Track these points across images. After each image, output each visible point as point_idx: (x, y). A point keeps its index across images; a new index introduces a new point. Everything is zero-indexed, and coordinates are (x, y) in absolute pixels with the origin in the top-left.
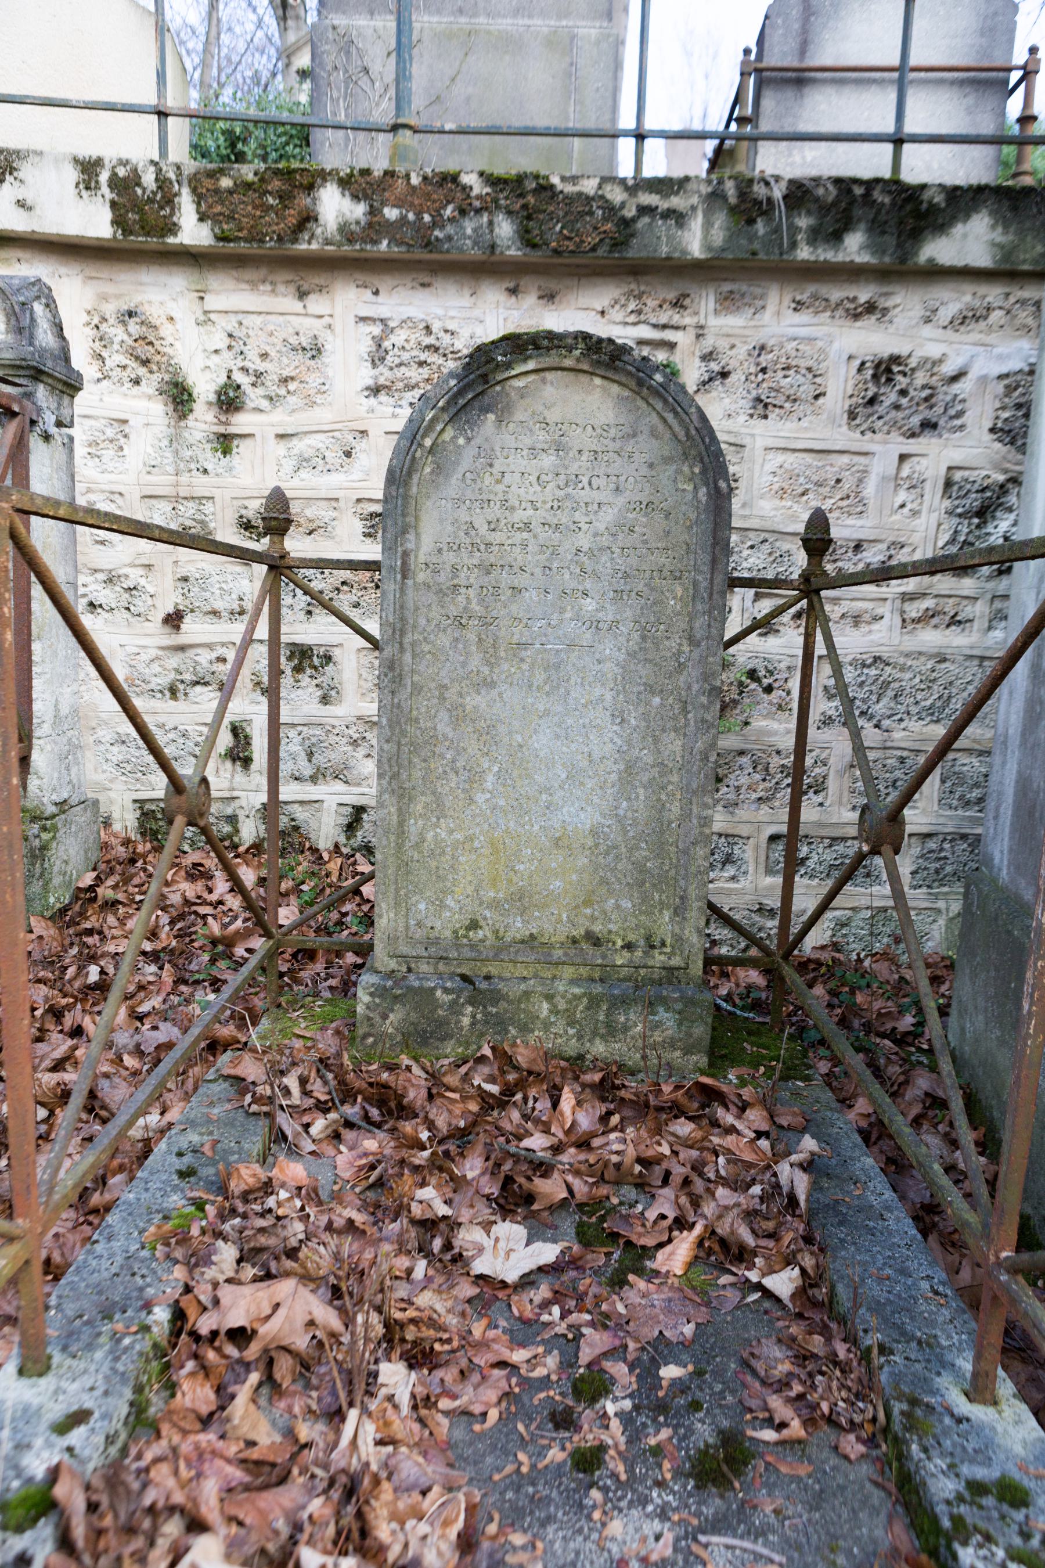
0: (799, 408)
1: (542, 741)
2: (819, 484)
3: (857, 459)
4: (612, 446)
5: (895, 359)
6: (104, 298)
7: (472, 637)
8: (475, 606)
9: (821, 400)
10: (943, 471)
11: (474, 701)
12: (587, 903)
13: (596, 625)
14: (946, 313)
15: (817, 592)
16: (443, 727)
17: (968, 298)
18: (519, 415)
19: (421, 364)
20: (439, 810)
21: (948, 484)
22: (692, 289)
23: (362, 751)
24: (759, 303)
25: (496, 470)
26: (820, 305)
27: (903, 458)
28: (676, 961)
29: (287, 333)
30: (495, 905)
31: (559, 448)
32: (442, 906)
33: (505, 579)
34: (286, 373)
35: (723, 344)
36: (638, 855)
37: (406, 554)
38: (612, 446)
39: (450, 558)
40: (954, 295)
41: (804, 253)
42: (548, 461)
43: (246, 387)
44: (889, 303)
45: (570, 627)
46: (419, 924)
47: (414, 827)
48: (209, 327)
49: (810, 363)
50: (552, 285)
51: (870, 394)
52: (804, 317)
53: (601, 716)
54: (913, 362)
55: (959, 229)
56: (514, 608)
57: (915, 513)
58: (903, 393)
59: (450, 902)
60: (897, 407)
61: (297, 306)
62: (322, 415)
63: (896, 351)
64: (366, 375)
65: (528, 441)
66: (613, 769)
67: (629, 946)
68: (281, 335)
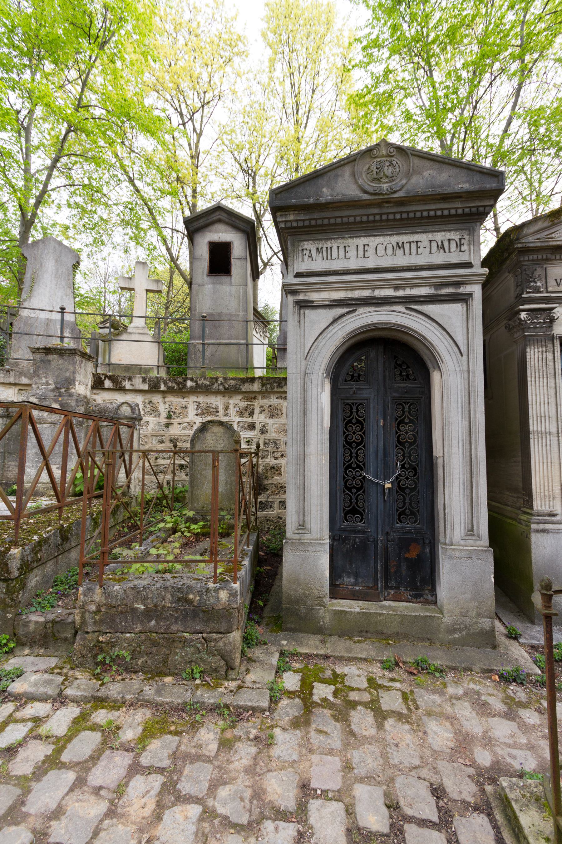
16: (199, 476)
22: (257, 395)
31: (215, 436)
41: (276, 390)
47: (194, 492)
64: (195, 412)
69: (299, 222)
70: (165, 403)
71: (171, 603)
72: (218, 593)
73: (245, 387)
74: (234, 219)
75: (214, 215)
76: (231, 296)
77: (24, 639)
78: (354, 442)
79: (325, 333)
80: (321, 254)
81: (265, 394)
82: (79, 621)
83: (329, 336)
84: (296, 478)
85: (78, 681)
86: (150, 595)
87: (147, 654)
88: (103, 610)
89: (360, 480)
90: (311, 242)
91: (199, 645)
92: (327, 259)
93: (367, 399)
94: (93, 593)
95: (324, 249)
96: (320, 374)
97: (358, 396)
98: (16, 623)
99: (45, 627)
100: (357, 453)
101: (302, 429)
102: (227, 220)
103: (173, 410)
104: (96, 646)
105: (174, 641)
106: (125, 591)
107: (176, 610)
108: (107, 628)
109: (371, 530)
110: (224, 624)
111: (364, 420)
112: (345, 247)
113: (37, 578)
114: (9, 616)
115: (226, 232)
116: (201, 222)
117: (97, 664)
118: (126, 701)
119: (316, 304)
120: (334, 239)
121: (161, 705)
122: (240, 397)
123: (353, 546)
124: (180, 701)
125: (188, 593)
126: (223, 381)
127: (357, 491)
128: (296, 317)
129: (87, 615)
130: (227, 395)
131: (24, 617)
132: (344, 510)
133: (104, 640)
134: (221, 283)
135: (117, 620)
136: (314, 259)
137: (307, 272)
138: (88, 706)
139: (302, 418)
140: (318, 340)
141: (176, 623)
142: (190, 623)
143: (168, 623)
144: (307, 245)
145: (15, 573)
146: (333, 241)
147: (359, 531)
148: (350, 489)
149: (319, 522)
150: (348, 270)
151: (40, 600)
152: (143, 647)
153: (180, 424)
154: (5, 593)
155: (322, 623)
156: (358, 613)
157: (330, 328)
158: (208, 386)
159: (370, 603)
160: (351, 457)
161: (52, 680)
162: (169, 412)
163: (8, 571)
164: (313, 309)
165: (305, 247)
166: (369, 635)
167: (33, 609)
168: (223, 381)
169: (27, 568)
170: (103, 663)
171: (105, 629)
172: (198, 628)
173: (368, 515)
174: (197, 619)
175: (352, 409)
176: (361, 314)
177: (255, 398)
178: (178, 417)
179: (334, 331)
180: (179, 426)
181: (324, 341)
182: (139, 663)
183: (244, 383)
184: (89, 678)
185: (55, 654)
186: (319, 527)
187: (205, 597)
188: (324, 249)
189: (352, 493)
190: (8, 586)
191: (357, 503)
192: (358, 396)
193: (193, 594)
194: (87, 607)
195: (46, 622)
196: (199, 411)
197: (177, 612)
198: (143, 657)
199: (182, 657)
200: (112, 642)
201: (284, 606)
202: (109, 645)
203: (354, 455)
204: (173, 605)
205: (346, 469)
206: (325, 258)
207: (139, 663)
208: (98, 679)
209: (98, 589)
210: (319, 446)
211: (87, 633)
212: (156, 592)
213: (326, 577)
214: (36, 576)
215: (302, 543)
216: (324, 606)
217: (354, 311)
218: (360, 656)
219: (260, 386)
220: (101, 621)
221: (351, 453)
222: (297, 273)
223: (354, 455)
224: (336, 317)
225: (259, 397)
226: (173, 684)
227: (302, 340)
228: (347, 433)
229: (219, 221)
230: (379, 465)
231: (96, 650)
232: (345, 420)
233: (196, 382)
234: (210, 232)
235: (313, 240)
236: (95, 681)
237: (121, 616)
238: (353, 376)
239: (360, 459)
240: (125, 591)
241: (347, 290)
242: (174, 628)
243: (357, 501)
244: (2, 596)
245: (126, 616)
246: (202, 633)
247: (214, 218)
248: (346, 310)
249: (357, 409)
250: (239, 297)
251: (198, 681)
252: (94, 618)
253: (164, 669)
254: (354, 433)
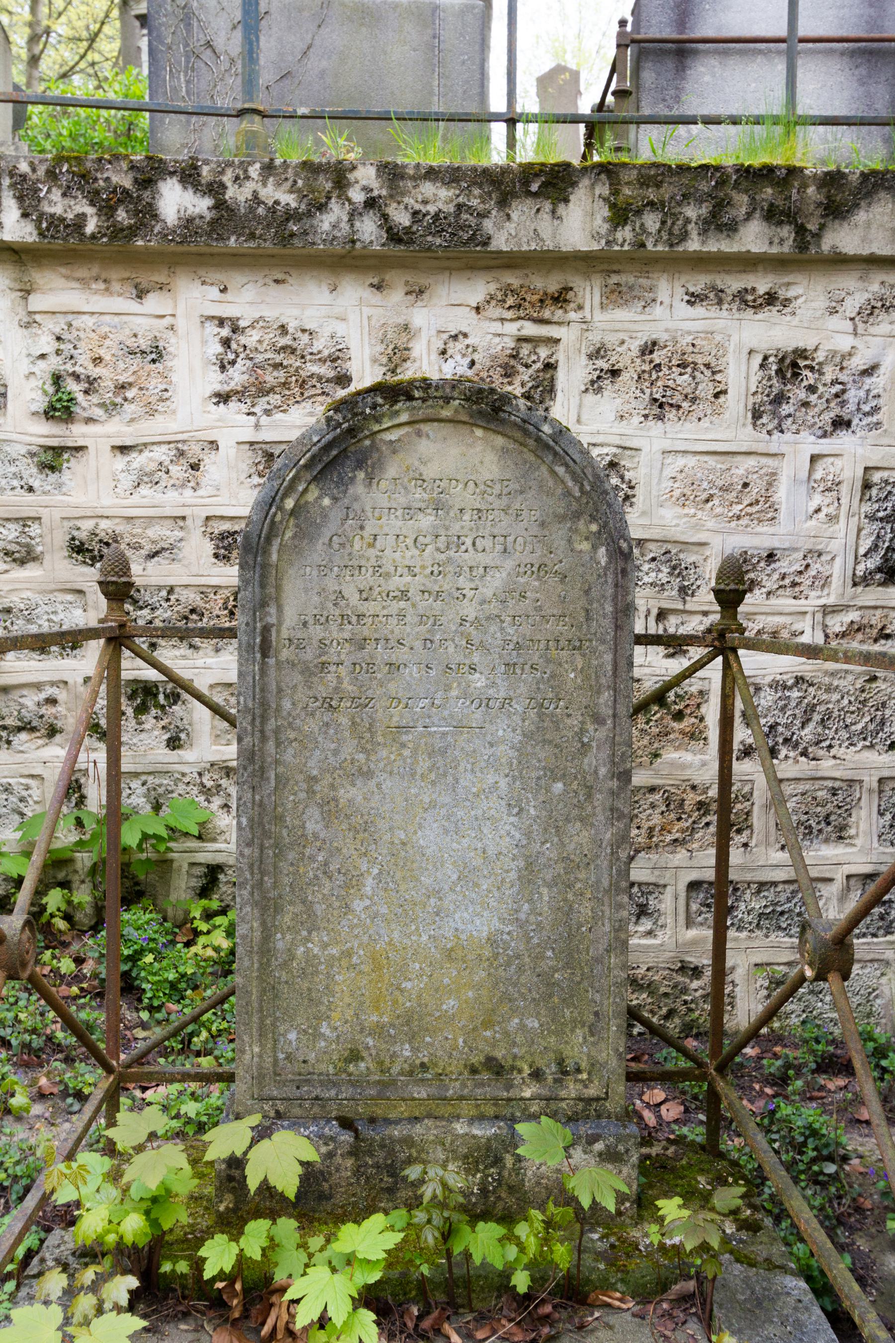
0: (700, 408)
2: (725, 489)
3: (764, 460)
4: (497, 503)
5: (801, 353)
7: (344, 721)
8: (346, 685)
9: (722, 399)
10: (860, 472)
11: (348, 793)
12: (487, 1024)
13: (486, 702)
14: (852, 305)
15: (734, 650)
17: (875, 287)
18: (392, 470)
19: (277, 366)
21: (867, 486)
23: (217, 801)
24: (649, 296)
25: (369, 530)
27: (814, 459)
28: (592, 1091)
29: (124, 335)
30: (379, 1031)
32: (317, 1035)
33: (381, 653)
34: (122, 379)
35: (611, 339)
36: (544, 966)
37: (266, 629)
38: (497, 503)
39: (316, 632)
40: (860, 284)
41: (694, 245)
42: (426, 521)
43: (80, 397)
44: (791, 294)
45: (458, 707)
46: (289, 1057)
47: (280, 942)
48: (34, 330)
49: (707, 359)
50: (424, 281)
51: (775, 391)
52: (699, 311)
53: (495, 806)
54: (820, 356)
55: (861, 216)
56: (392, 687)
57: (832, 519)
58: (812, 389)
59: (325, 1029)
60: (806, 404)
61: (133, 306)
63: (801, 345)
64: (215, 381)
65: (402, 500)
66: (512, 868)
67: (537, 1075)
68: (116, 337)
70: (30, 323)
103: (85, 366)
126: (379, 190)
130: (398, 280)
153: (123, 449)
158: (291, 215)
162: (57, 379)
168: (379, 190)
177: (560, 299)
178: (111, 408)
180: (120, 462)
183: (503, 203)
196: (238, 376)
233: (215, 189)
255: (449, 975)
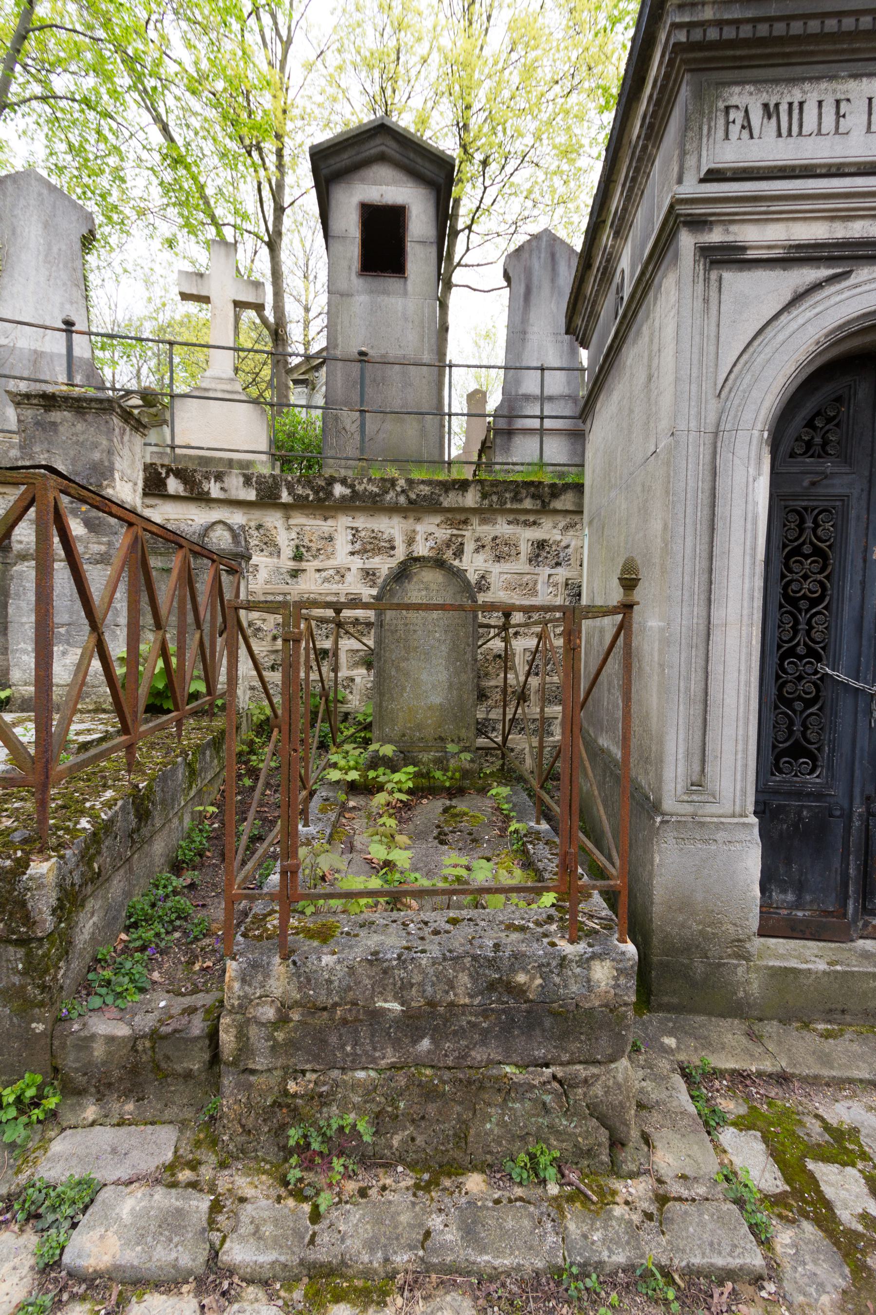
1: (424, 676)
5: (545, 541)
6: (250, 520)
11: (403, 665)
14: (561, 525)
20: (392, 699)
21: (567, 585)
22: (471, 516)
23: (348, 691)
26: (517, 522)
27: (550, 576)
29: (320, 533)
30: (410, 728)
31: (427, 589)
35: (482, 535)
39: (395, 622)
41: (508, 506)
42: (424, 593)
47: (384, 704)
50: (420, 515)
52: (511, 527)
53: (441, 668)
55: (563, 497)
57: (556, 595)
58: (548, 553)
61: (323, 523)
62: (331, 563)
64: (350, 548)
66: (446, 685)
69: (726, 29)
70: (288, 528)
71: (471, 996)
72: (589, 969)
73: (450, 500)
74: (412, 155)
75: (372, 143)
76: (406, 319)
77: (80, 1080)
78: (804, 597)
79: (770, 332)
80: (774, 120)
81: (485, 513)
82: (233, 1045)
83: (781, 337)
84: (688, 679)
85: (249, 1207)
86: (417, 978)
87: (413, 1121)
88: (295, 1016)
89: (814, 684)
90: (749, 88)
91: (548, 1098)
92: (790, 134)
93: (844, 499)
94: (267, 976)
95: (784, 108)
96: (756, 433)
97: (821, 490)
98: (56, 1043)
99: (134, 1049)
100: (809, 623)
101: (705, 564)
102: (397, 156)
103: (306, 542)
104: (280, 1106)
105: (482, 1088)
106: (351, 968)
107: (485, 1013)
108: (308, 1061)
109: (838, 792)
110: (604, 1041)
111: (829, 547)
112: (838, 102)
113: (95, 919)
114: (39, 1027)
115: (394, 183)
116: (345, 159)
117: (287, 1152)
118: (395, 1272)
119: (751, 254)
120: (811, 79)
121: (492, 1279)
122: (438, 519)
123: (797, 826)
124: (540, 1264)
125: (512, 970)
126: (406, 487)
127: (807, 707)
128: (700, 287)
129: (253, 1031)
130: (412, 515)
131: (76, 1027)
132: (774, 747)
133: (300, 1090)
134: (386, 292)
135: (333, 1040)
136: (756, 133)
137: (735, 170)
138: (298, 1294)
139: (706, 539)
140: (751, 349)
141: (484, 1043)
142: (520, 1043)
143: (464, 1043)
144: (739, 96)
145: (47, 922)
146: (807, 86)
147: (809, 794)
148: (789, 703)
149: (739, 777)
150: (840, 165)
151: (107, 974)
152: (402, 1105)
153: (319, 571)
154: (25, 973)
155: (741, 994)
156: (824, 972)
157: (784, 318)
158: (377, 495)
159: (833, 945)
160: (796, 632)
161: (179, 1211)
162: (297, 547)
163: (28, 920)
164: (741, 270)
165: (734, 101)
166: (848, 1018)
167: (96, 1002)
168: (406, 487)
169: (72, 904)
170: (304, 1148)
171: (299, 1061)
172: (540, 1053)
173: (830, 759)
174: (538, 1032)
175: (803, 521)
176: (865, 283)
177: (465, 522)
178: (315, 557)
179: (794, 325)
180: (317, 575)
181: (768, 350)
182: (395, 1143)
183: (446, 492)
184: (273, 1193)
185: (166, 1116)
186: (738, 787)
187: (557, 980)
188: (784, 108)
189: (794, 711)
190: (29, 955)
191: (804, 734)
192: (821, 490)
193: (528, 972)
194: (251, 1012)
195: (135, 1039)
196: (358, 546)
197: (486, 1017)
198: (405, 1128)
199: (501, 1124)
200: (321, 1095)
201: (655, 959)
202: (315, 1103)
203: (803, 626)
204: (476, 1001)
205: (782, 658)
206: (784, 131)
207: (395, 1143)
208: (300, 1196)
209: (277, 966)
210: (745, 604)
211: (253, 1072)
212: (431, 971)
213: (754, 898)
214: (93, 914)
215: (702, 824)
216: (747, 959)
217: (846, 275)
218: (857, 1074)
219: (478, 499)
220: (292, 1045)
221: (796, 622)
222: (710, 171)
223: (803, 626)
224: (801, 290)
225: (475, 520)
226: (497, 1202)
227: (712, 348)
228: (790, 577)
229: (382, 158)
230: (864, 649)
231: (282, 1115)
232: (785, 546)
233: (352, 486)
234: (363, 181)
235: (754, 82)
236: (291, 1202)
237: (343, 1031)
238: (809, 444)
239: (817, 636)
240: (351, 968)
241: (832, 219)
242: (478, 1055)
243: (806, 728)
244: (16, 980)
245: (356, 1031)
246: (547, 1066)
247: (373, 151)
248: (825, 272)
249: (815, 521)
250: (422, 322)
251: (553, 1189)
252: (270, 1037)
253: (458, 1154)
254: (805, 577)
255: (429, 714)
